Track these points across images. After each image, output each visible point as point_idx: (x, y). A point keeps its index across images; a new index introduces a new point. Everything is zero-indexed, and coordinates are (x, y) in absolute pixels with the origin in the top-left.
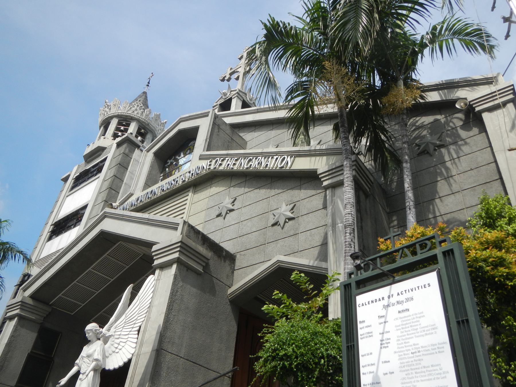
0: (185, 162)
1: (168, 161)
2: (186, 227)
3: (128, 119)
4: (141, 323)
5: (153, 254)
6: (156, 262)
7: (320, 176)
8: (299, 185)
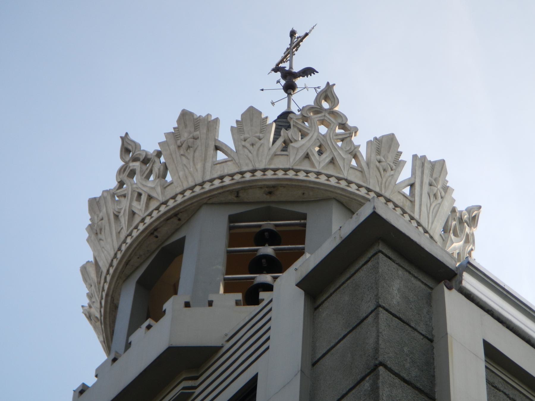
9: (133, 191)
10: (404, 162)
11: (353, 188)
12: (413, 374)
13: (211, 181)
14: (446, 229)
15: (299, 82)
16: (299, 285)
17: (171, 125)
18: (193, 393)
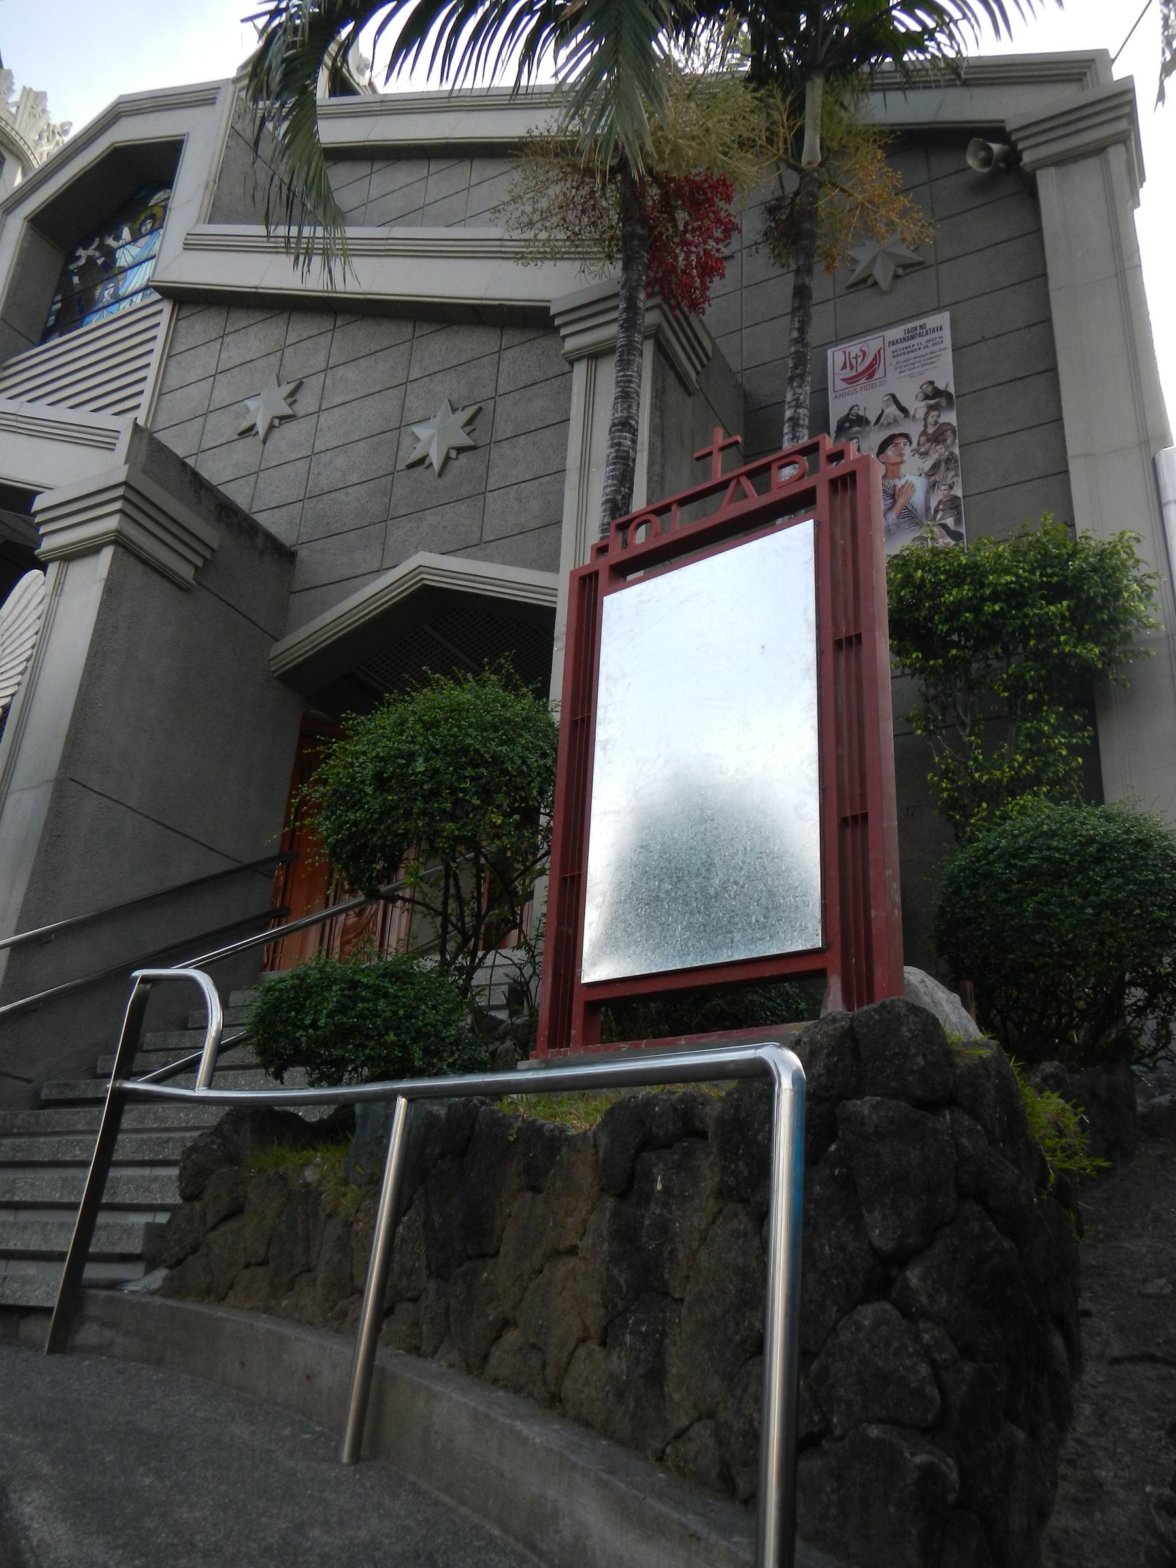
0: (138, 260)
1: (78, 254)
2: (144, 449)
4: (8, 699)
5: (38, 519)
6: (47, 544)
7: (557, 322)
8: (496, 350)
10: (14, 91)
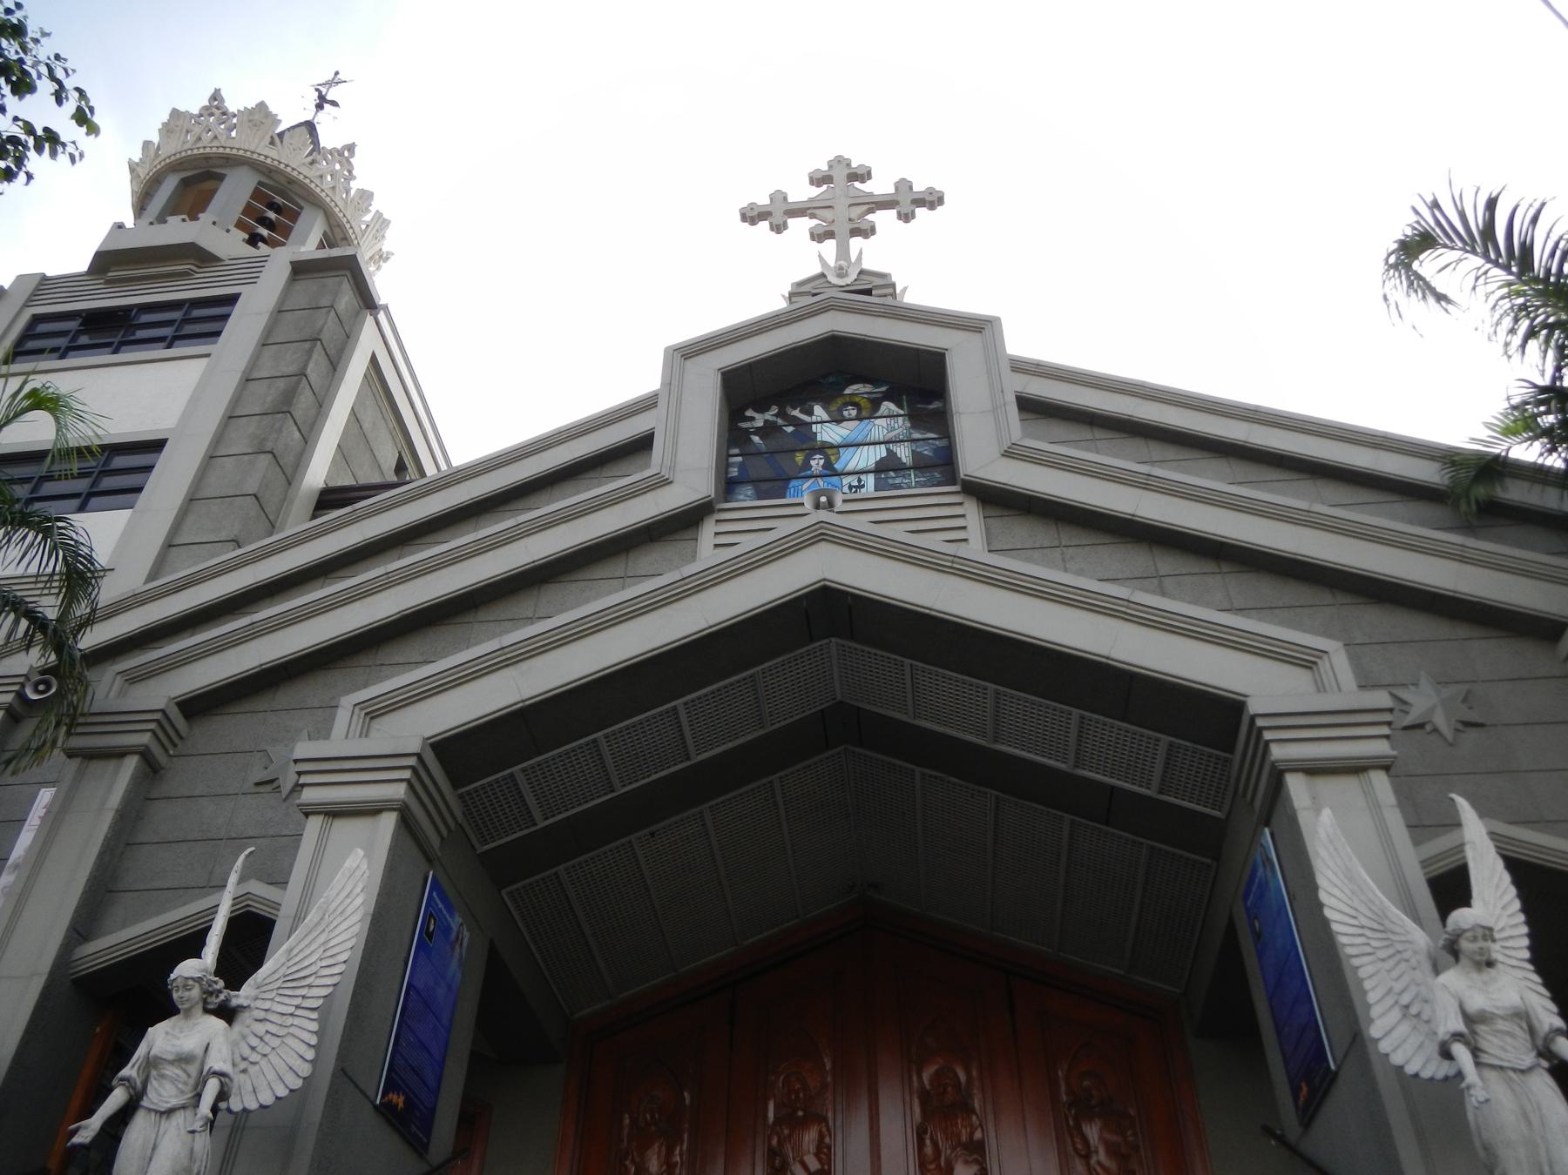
3: (291, 190)
9: (207, 126)
11: (337, 210)
12: (332, 352)
13: (259, 154)
14: (371, 258)
15: (327, 106)
16: (291, 263)
17: (251, 104)
18: (192, 275)
